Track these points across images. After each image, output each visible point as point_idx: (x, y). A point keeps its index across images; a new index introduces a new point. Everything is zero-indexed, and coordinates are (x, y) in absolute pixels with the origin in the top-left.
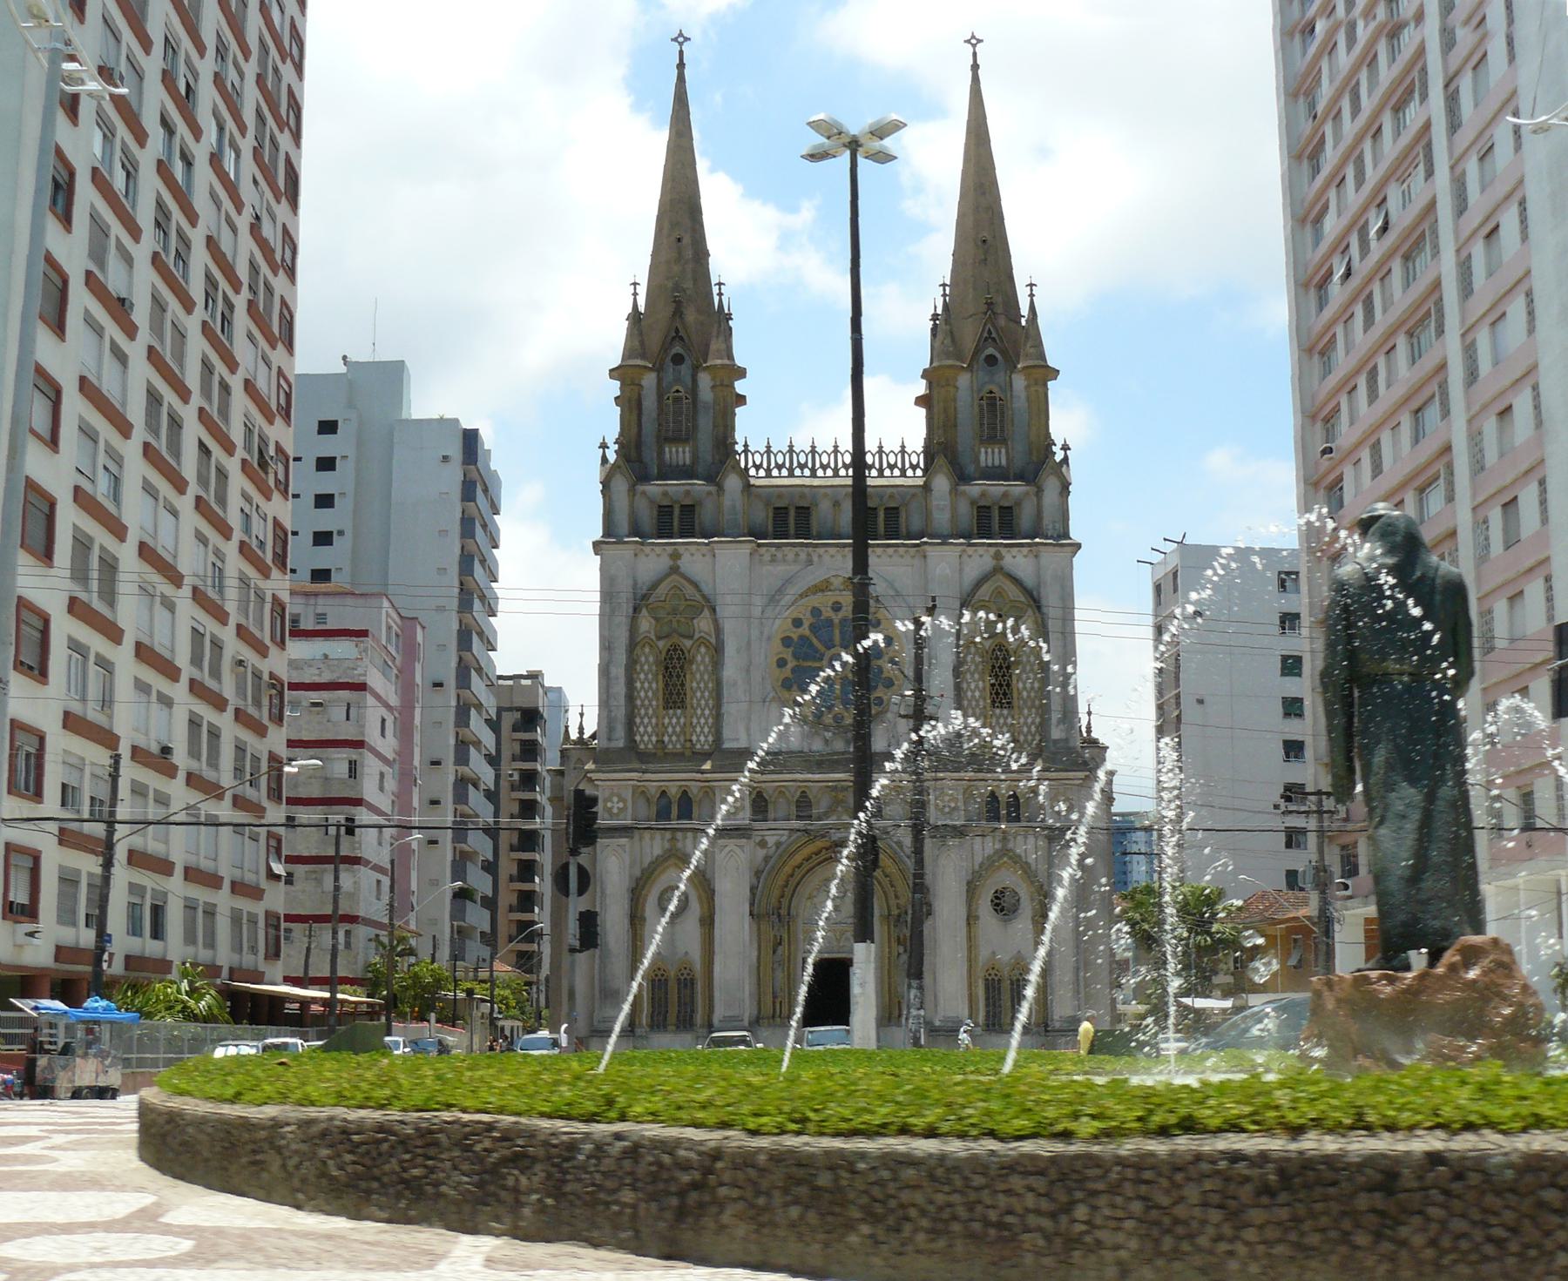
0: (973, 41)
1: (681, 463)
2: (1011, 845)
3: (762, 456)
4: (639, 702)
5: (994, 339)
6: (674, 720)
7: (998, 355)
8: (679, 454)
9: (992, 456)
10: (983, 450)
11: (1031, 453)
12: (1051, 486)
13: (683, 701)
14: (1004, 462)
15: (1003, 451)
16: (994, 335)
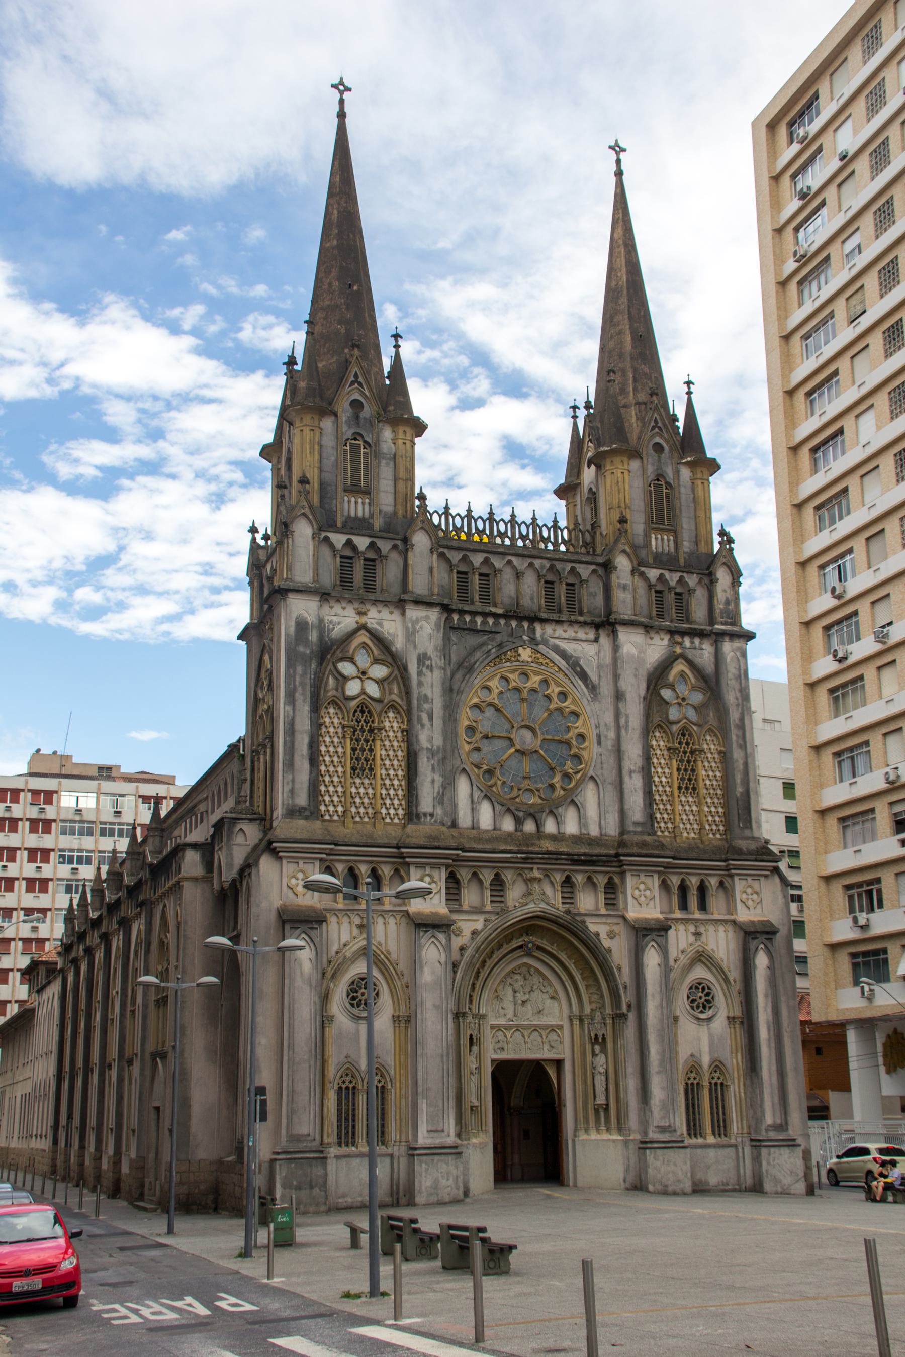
0: (617, 149)
1: (353, 514)
2: (703, 938)
3: (440, 516)
4: (323, 768)
5: (660, 428)
6: (360, 788)
7: (665, 445)
8: (356, 507)
9: (660, 543)
10: (653, 536)
11: (697, 543)
12: (723, 576)
13: (371, 769)
14: (672, 550)
15: (672, 538)
16: (660, 424)
